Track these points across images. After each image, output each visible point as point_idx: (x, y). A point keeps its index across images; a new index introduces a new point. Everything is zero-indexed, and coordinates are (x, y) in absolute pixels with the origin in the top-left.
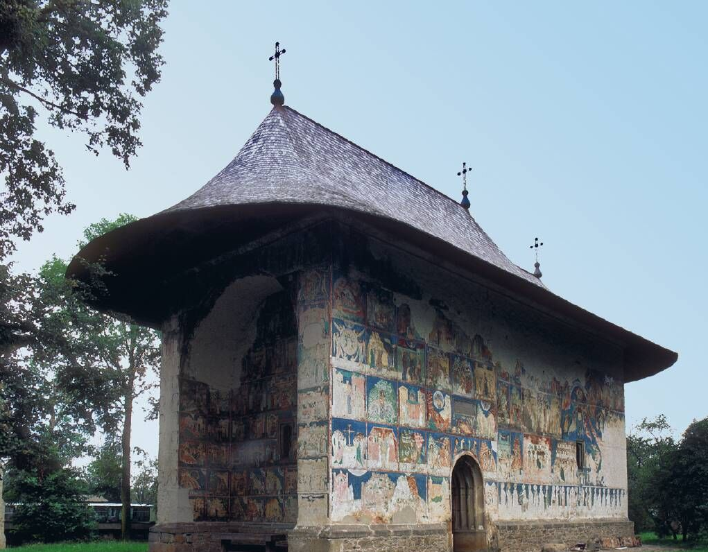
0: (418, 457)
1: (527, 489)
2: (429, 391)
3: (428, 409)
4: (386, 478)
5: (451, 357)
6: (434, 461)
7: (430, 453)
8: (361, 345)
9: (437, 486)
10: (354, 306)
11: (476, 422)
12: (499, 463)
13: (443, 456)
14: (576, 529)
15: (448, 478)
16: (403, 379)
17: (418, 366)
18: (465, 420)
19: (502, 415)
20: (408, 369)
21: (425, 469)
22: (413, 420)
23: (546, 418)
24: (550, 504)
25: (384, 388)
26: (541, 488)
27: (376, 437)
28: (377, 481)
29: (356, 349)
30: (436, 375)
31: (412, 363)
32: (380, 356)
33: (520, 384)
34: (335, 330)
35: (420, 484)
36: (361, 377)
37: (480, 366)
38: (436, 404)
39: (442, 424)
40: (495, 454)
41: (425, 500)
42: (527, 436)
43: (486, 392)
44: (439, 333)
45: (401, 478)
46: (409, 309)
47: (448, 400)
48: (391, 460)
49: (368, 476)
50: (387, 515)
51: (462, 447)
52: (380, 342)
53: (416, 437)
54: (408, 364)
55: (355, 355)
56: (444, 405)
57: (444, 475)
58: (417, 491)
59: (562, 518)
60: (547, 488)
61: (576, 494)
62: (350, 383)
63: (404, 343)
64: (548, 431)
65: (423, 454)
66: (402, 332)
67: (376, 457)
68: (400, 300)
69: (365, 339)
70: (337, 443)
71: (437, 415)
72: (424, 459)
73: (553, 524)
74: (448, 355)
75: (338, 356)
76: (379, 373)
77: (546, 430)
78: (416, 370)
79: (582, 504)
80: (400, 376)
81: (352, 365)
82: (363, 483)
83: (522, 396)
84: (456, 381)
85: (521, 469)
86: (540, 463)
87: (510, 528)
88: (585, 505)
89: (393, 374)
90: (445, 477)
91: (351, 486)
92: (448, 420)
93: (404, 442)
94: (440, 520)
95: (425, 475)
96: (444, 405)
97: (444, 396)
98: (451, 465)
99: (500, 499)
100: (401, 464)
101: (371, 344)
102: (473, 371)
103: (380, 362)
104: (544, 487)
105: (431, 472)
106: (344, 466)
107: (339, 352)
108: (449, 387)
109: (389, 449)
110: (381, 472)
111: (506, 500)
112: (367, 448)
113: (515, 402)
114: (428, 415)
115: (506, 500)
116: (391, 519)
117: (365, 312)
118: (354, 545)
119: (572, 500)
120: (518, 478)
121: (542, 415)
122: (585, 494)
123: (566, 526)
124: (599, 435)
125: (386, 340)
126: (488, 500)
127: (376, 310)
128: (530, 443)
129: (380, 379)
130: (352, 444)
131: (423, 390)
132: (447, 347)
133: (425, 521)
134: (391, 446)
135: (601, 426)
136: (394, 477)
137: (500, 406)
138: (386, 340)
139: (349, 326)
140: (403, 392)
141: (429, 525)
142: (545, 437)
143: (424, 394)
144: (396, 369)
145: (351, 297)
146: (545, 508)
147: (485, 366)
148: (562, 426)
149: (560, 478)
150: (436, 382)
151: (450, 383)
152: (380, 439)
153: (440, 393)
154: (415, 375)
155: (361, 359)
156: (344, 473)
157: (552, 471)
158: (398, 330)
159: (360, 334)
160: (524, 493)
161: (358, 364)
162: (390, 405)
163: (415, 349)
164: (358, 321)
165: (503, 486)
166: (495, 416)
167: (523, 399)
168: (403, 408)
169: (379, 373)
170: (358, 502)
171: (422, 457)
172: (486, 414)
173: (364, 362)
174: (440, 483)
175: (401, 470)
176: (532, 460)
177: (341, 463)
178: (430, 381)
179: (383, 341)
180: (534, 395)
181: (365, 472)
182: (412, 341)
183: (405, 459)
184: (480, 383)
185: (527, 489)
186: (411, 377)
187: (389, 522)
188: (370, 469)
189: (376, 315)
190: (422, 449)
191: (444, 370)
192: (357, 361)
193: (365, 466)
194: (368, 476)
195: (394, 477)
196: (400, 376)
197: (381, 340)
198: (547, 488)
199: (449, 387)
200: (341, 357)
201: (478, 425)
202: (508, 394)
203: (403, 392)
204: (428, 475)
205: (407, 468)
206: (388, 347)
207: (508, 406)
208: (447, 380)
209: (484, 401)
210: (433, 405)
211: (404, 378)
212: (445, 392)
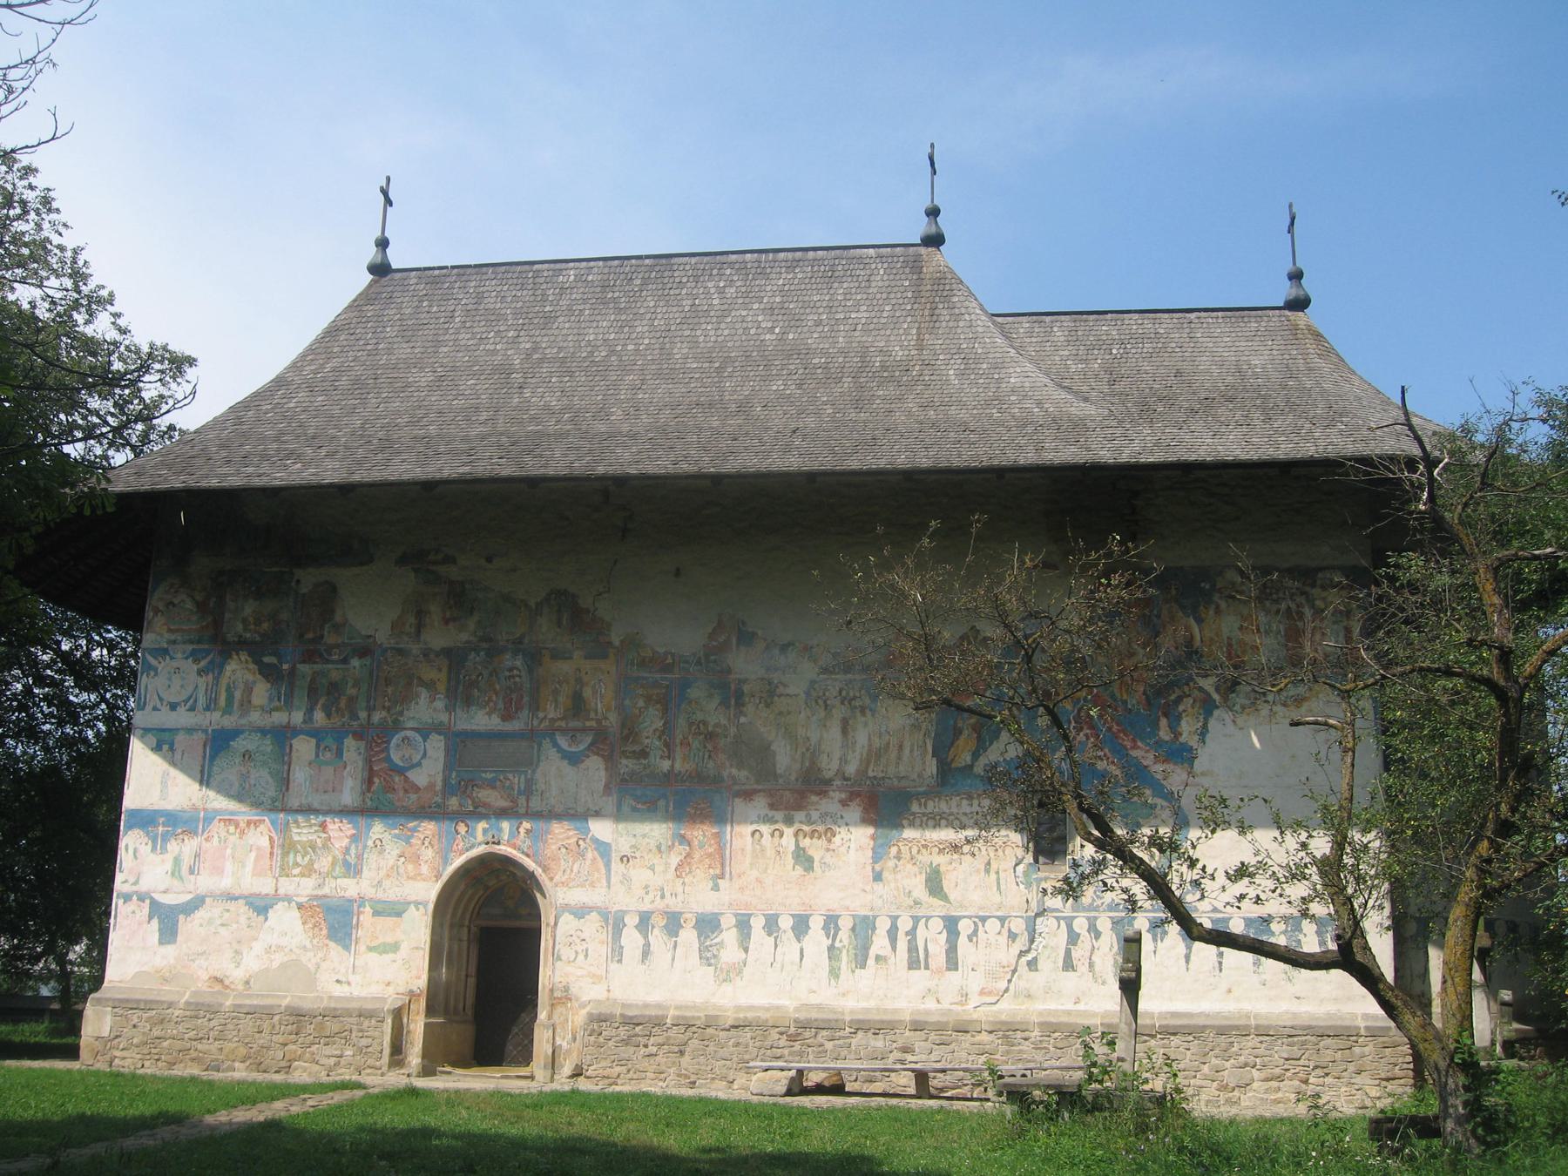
0: (333, 864)
1: (743, 925)
2: (376, 739)
3: (371, 769)
4: (241, 908)
5: (454, 658)
6: (382, 873)
7: (371, 859)
8: (202, 682)
9: (390, 921)
10: (194, 618)
11: (530, 783)
12: (616, 866)
13: (416, 859)
14: (984, 1037)
15: (425, 904)
16: (305, 722)
17: (351, 691)
18: (494, 780)
19: (644, 754)
20: (321, 701)
21: (350, 888)
22: (326, 797)
23: (893, 732)
24: (863, 966)
25: (251, 747)
26: (816, 923)
27: (223, 834)
28: (217, 911)
29: (190, 689)
30: (406, 698)
31: (334, 689)
32: (249, 690)
33: (729, 671)
34: (149, 668)
35: (337, 921)
36: (201, 735)
37: (556, 655)
38: (396, 757)
39: (414, 797)
40: (603, 849)
41: (347, 948)
42: (748, 795)
43: (578, 706)
44: (420, 614)
45: (280, 906)
46: (334, 589)
47: (436, 747)
48: (257, 873)
49: (196, 903)
50: (237, 975)
51: (480, 837)
52: (252, 666)
53: (330, 826)
54: (326, 693)
55: (186, 702)
56: (425, 754)
57: (413, 898)
58: (325, 932)
59: (931, 1005)
60: (845, 924)
61: (1012, 936)
62: (172, 749)
63: (309, 657)
64: (862, 772)
65: (352, 859)
66: (310, 635)
67: (218, 871)
68: (308, 578)
69: (216, 668)
70: (131, 851)
71: (397, 779)
72: (352, 870)
73: (848, 1018)
74: (447, 652)
75: (149, 708)
76: (243, 721)
77: (851, 769)
78: (343, 703)
79: (1050, 962)
80: (298, 717)
81: (182, 718)
82: (182, 917)
83: (733, 697)
84: (468, 702)
85: (722, 876)
86: (810, 860)
87: (630, 1022)
88: (1068, 965)
89: (279, 718)
90: (417, 904)
91: (155, 922)
92: (431, 786)
93: (296, 838)
94: (391, 990)
95: (351, 901)
96: (425, 754)
97: (425, 738)
98: (438, 877)
99: (617, 953)
100: (282, 880)
101: (228, 674)
102: (530, 671)
103: (246, 705)
104: (831, 923)
105: (370, 892)
106: (143, 886)
107: (153, 701)
108: (444, 717)
109: (253, 855)
110: (231, 897)
111: (646, 953)
112: (197, 855)
113: (699, 716)
114: (370, 782)
115: (646, 953)
116: (247, 983)
117: (217, 624)
118: (135, 1020)
119: (987, 954)
120: (699, 896)
121: (835, 732)
122: (1073, 938)
123: (917, 1027)
124: (1182, 755)
125: (266, 659)
126: (566, 953)
127: (244, 614)
128: (766, 811)
129: (242, 732)
130: (164, 850)
131: (358, 736)
132: (438, 637)
133: (339, 991)
134: (258, 849)
135: (1188, 727)
136: (261, 906)
137: (630, 731)
138: (266, 659)
139: (180, 655)
140: (303, 747)
141: (351, 999)
142: (840, 789)
143: (362, 744)
144: (289, 706)
145: (189, 605)
146: (834, 973)
147: (576, 654)
148: (941, 752)
149: (920, 892)
150: (401, 713)
151: (450, 709)
152: (233, 839)
153: (409, 733)
154: (338, 710)
155: (202, 701)
156: (141, 899)
157: (878, 877)
158: (301, 636)
159: (203, 663)
160: (729, 936)
161: (192, 714)
162: (264, 773)
163: (345, 661)
164: (199, 642)
165: (632, 921)
166: (609, 759)
167: (740, 704)
168: (300, 775)
169: (243, 721)
170: (170, 950)
171: (346, 864)
172: (574, 759)
173: (208, 708)
174: (399, 914)
175: (281, 891)
176: (770, 853)
177: (136, 883)
178: (384, 713)
179: (258, 662)
180: (796, 687)
181: (190, 897)
182: (337, 646)
183: (296, 871)
184: (556, 692)
185: (743, 925)
186: (329, 716)
187: (240, 987)
188: (202, 890)
189: (244, 621)
190: (347, 849)
191: (430, 686)
192: (192, 709)
193: (191, 887)
194: (196, 903)
195: (261, 906)
196: (298, 717)
197: (255, 662)
198: (845, 924)
199: (444, 717)
200: (155, 709)
201: (541, 786)
202: (667, 702)
203: (303, 747)
204: (362, 900)
205: (304, 887)
206: (269, 673)
207: (666, 733)
208: (440, 704)
209: (564, 731)
210: (388, 759)
211: (309, 717)
212: (425, 733)
